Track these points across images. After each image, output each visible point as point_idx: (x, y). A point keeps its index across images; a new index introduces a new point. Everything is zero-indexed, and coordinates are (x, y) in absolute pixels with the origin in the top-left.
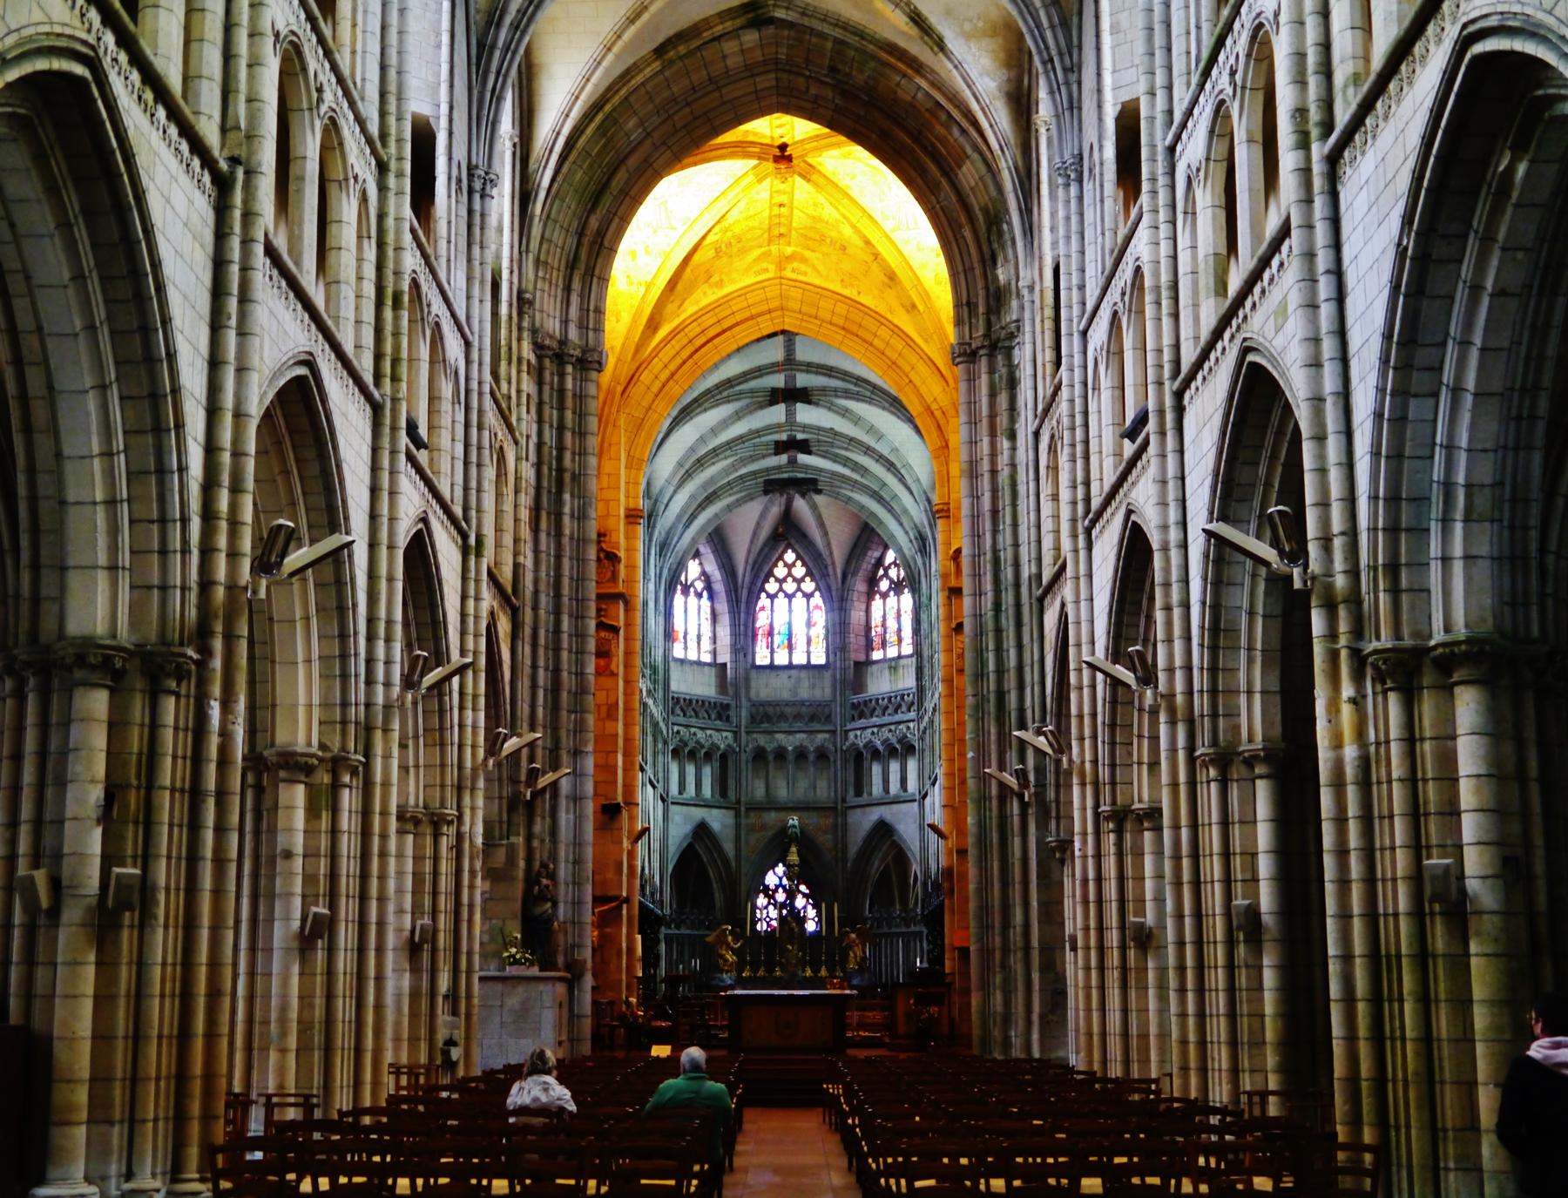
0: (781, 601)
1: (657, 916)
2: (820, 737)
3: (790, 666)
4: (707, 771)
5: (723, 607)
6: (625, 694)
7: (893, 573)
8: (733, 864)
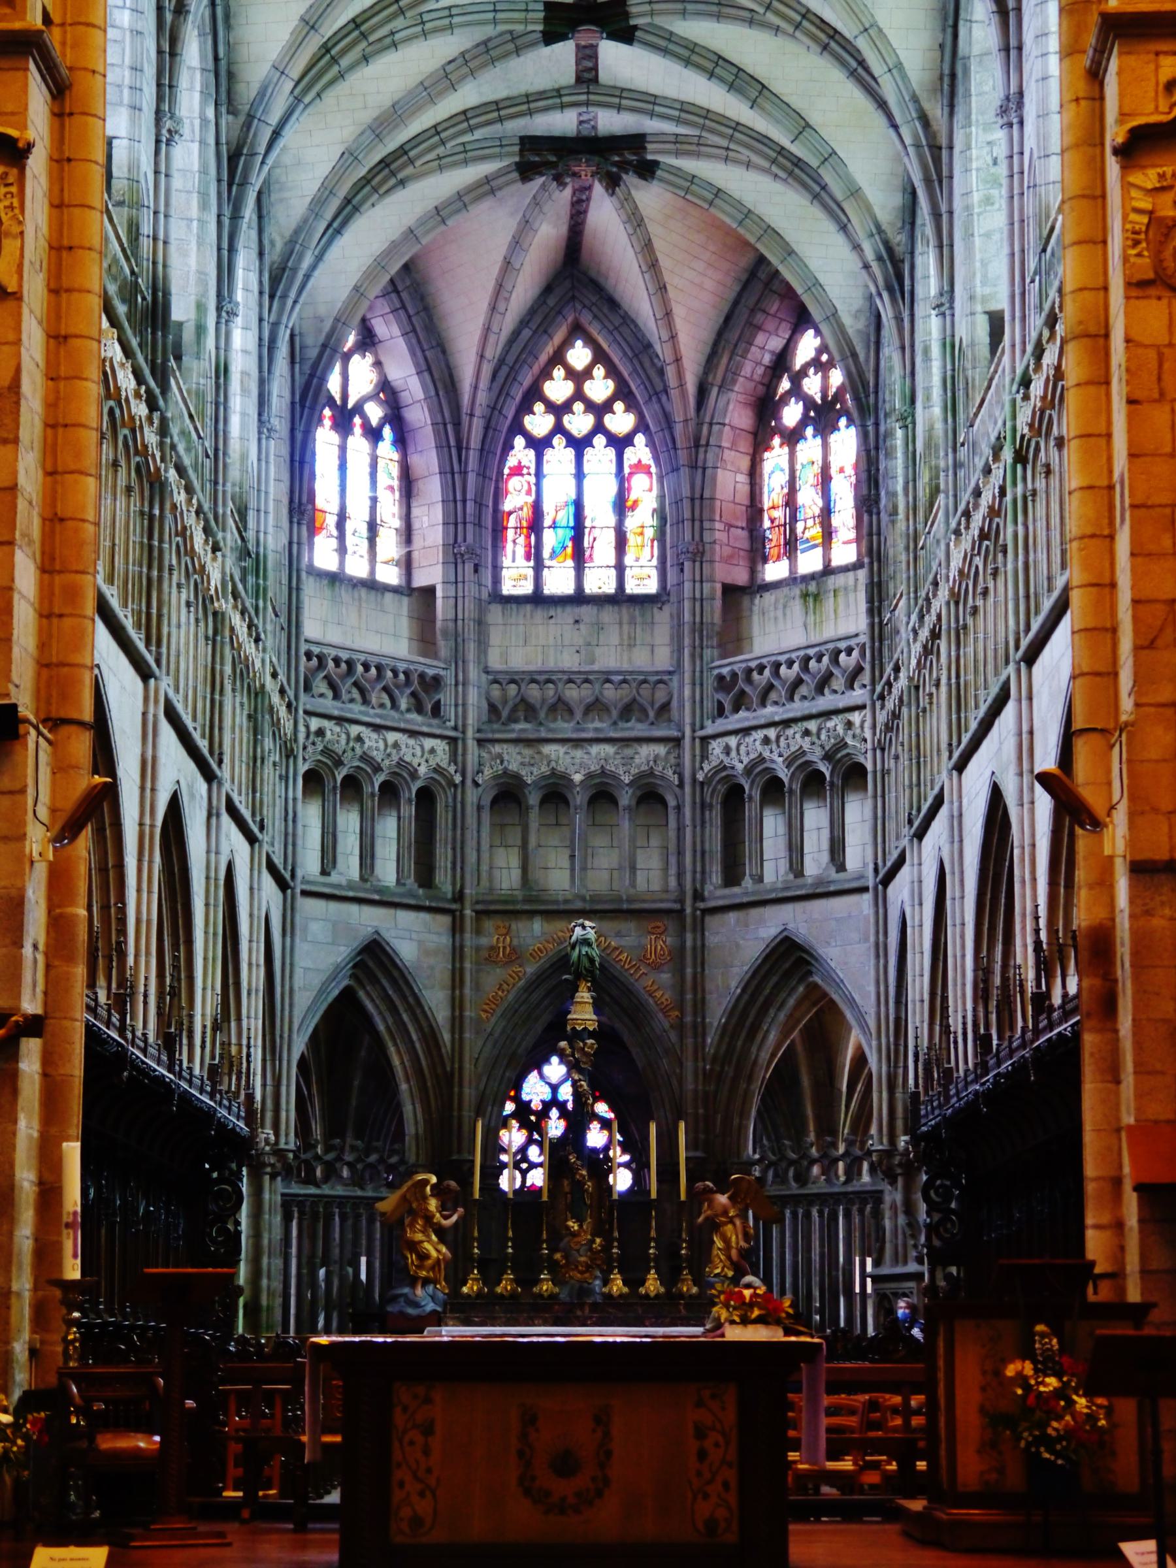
0: (560, 456)
1: (227, 1134)
2: (645, 753)
3: (579, 598)
4: (388, 828)
5: (427, 460)
6: (52, 376)
7: (812, 385)
8: (447, 1036)
